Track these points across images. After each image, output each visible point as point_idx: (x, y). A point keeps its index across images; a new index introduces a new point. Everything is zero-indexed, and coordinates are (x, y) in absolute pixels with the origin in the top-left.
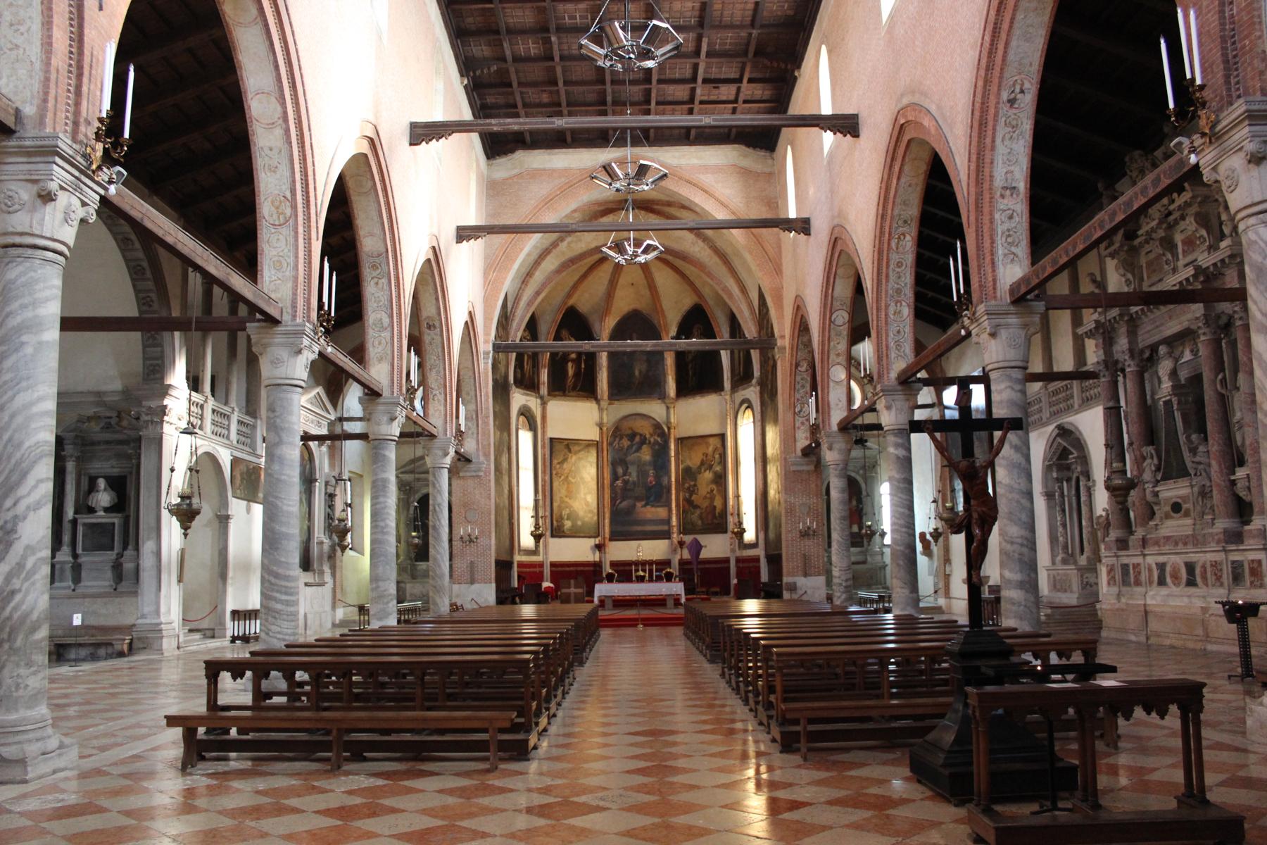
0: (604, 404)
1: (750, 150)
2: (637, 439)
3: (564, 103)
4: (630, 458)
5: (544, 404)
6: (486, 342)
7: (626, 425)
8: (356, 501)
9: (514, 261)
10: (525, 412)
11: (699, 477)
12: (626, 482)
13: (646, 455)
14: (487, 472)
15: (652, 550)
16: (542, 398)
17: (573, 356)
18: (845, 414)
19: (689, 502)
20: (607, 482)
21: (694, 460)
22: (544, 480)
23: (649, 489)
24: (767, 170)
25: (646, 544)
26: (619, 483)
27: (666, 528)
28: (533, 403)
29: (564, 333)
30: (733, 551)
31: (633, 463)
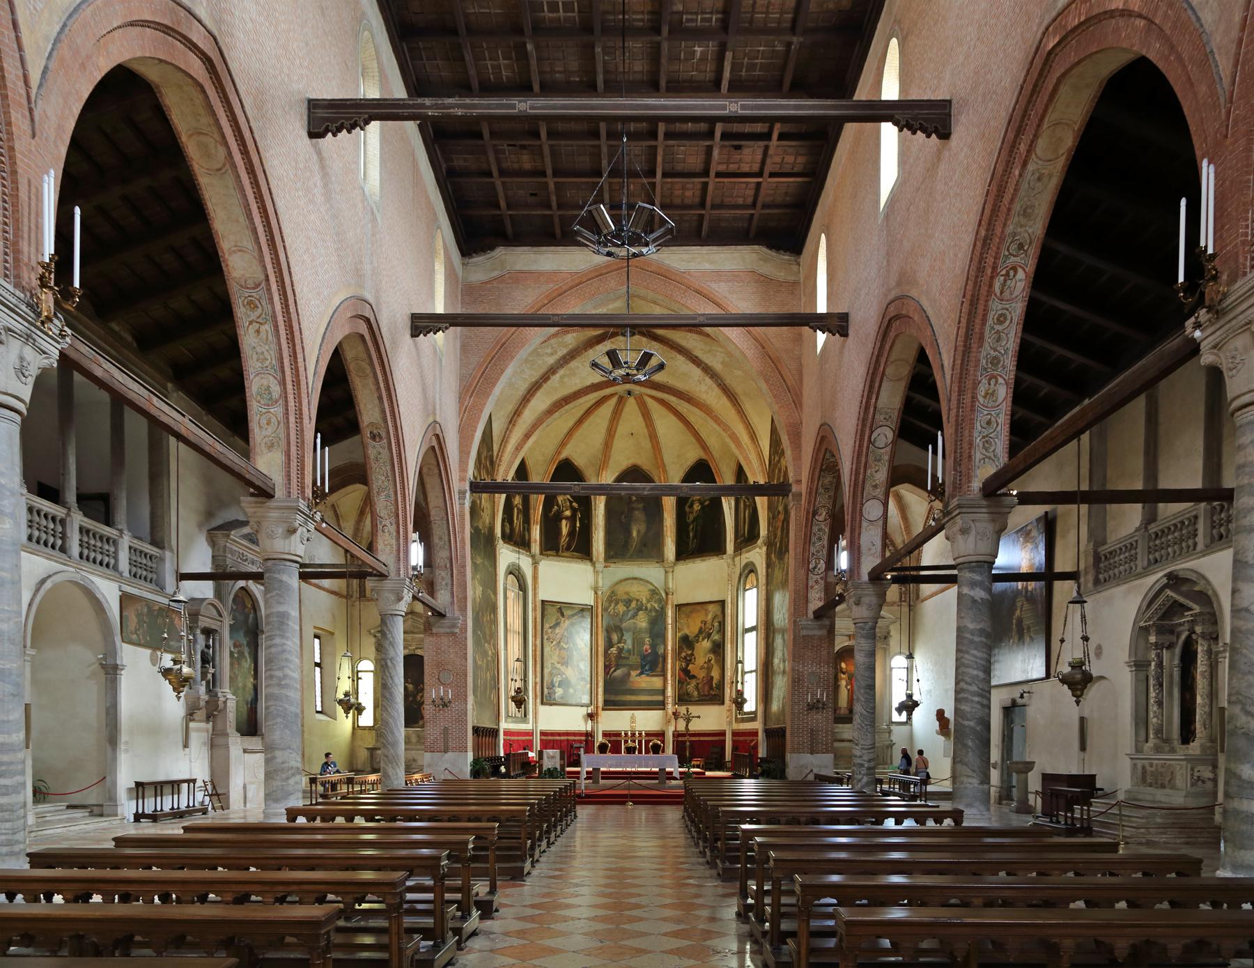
0: (600, 566)
1: (773, 253)
2: (633, 605)
3: (549, 172)
4: (624, 625)
5: (535, 564)
6: (462, 479)
7: (621, 590)
8: (327, 661)
9: (494, 385)
10: (515, 572)
11: (697, 645)
12: (620, 650)
13: (642, 622)
14: (464, 630)
15: (647, 721)
16: (533, 557)
17: (568, 513)
18: (879, 561)
19: (685, 671)
20: (601, 649)
21: (692, 628)
23: (644, 657)
24: (791, 278)
25: (639, 714)
26: (614, 650)
27: (660, 698)
28: (525, 563)
30: (730, 723)
31: (628, 630)
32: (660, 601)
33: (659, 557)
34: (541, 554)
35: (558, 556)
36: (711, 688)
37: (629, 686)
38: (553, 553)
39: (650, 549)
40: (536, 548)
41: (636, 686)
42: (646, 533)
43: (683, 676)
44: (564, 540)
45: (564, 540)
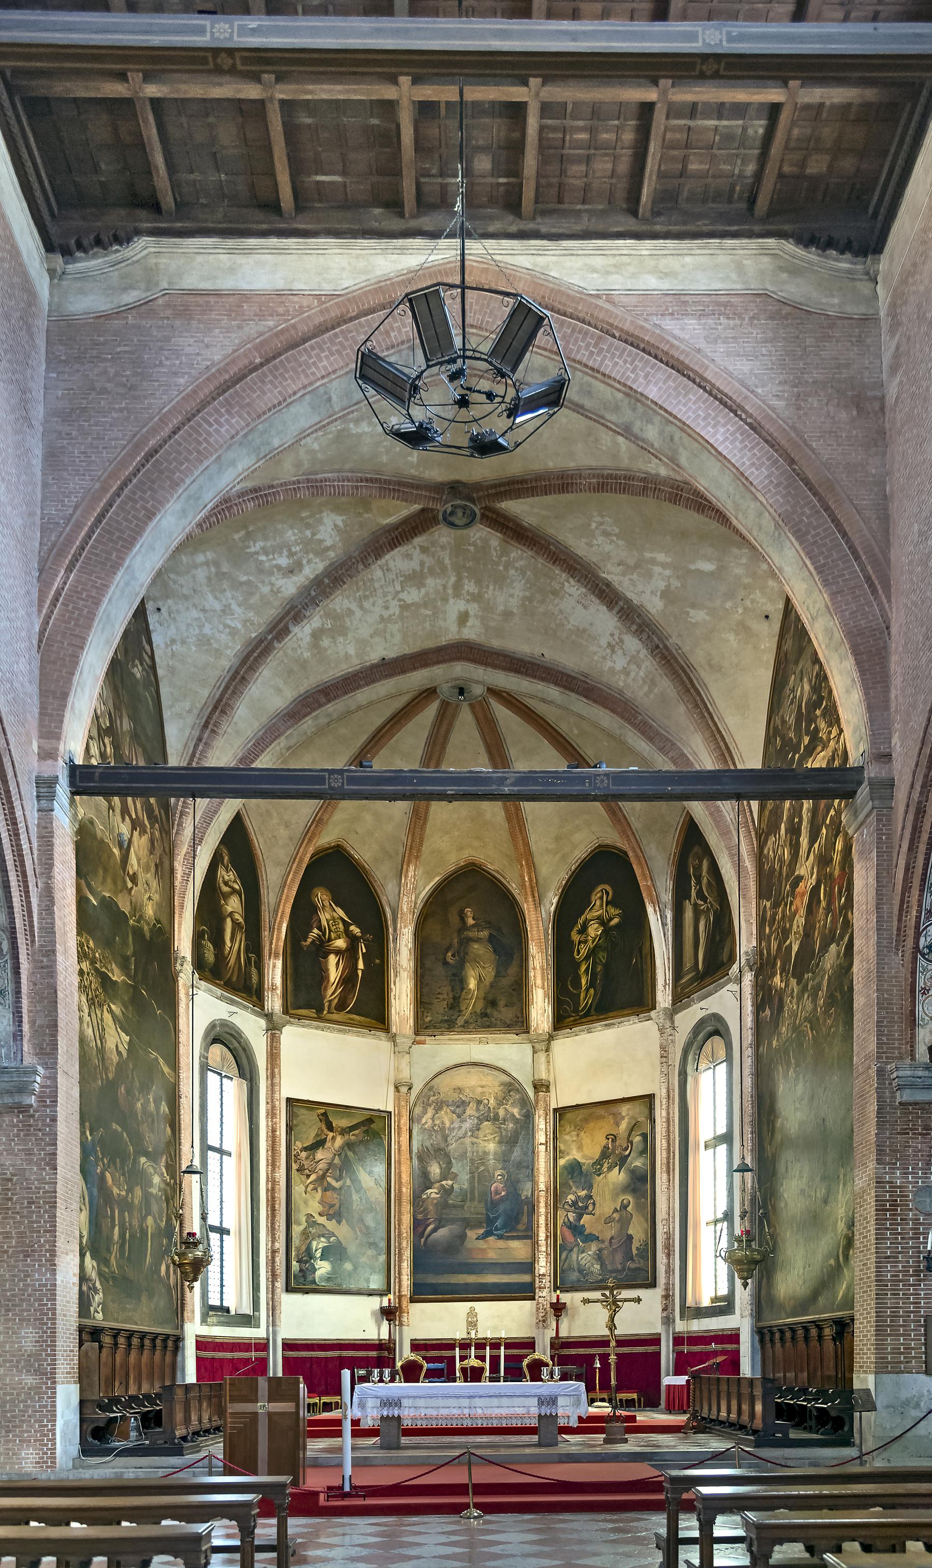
7: (446, 1084)
12: (447, 1192)
15: (502, 1319)
22: (272, 1181)
23: (493, 1205)
26: (433, 1193)
27: (526, 1278)
28: (251, 1027)
29: (321, 896)
30: (668, 1321)
33: (519, 1023)
34: (286, 1011)
35: (319, 1018)
36: (629, 1257)
37: (461, 1258)
41: (478, 1258)
44: (332, 992)
45: (332, 992)
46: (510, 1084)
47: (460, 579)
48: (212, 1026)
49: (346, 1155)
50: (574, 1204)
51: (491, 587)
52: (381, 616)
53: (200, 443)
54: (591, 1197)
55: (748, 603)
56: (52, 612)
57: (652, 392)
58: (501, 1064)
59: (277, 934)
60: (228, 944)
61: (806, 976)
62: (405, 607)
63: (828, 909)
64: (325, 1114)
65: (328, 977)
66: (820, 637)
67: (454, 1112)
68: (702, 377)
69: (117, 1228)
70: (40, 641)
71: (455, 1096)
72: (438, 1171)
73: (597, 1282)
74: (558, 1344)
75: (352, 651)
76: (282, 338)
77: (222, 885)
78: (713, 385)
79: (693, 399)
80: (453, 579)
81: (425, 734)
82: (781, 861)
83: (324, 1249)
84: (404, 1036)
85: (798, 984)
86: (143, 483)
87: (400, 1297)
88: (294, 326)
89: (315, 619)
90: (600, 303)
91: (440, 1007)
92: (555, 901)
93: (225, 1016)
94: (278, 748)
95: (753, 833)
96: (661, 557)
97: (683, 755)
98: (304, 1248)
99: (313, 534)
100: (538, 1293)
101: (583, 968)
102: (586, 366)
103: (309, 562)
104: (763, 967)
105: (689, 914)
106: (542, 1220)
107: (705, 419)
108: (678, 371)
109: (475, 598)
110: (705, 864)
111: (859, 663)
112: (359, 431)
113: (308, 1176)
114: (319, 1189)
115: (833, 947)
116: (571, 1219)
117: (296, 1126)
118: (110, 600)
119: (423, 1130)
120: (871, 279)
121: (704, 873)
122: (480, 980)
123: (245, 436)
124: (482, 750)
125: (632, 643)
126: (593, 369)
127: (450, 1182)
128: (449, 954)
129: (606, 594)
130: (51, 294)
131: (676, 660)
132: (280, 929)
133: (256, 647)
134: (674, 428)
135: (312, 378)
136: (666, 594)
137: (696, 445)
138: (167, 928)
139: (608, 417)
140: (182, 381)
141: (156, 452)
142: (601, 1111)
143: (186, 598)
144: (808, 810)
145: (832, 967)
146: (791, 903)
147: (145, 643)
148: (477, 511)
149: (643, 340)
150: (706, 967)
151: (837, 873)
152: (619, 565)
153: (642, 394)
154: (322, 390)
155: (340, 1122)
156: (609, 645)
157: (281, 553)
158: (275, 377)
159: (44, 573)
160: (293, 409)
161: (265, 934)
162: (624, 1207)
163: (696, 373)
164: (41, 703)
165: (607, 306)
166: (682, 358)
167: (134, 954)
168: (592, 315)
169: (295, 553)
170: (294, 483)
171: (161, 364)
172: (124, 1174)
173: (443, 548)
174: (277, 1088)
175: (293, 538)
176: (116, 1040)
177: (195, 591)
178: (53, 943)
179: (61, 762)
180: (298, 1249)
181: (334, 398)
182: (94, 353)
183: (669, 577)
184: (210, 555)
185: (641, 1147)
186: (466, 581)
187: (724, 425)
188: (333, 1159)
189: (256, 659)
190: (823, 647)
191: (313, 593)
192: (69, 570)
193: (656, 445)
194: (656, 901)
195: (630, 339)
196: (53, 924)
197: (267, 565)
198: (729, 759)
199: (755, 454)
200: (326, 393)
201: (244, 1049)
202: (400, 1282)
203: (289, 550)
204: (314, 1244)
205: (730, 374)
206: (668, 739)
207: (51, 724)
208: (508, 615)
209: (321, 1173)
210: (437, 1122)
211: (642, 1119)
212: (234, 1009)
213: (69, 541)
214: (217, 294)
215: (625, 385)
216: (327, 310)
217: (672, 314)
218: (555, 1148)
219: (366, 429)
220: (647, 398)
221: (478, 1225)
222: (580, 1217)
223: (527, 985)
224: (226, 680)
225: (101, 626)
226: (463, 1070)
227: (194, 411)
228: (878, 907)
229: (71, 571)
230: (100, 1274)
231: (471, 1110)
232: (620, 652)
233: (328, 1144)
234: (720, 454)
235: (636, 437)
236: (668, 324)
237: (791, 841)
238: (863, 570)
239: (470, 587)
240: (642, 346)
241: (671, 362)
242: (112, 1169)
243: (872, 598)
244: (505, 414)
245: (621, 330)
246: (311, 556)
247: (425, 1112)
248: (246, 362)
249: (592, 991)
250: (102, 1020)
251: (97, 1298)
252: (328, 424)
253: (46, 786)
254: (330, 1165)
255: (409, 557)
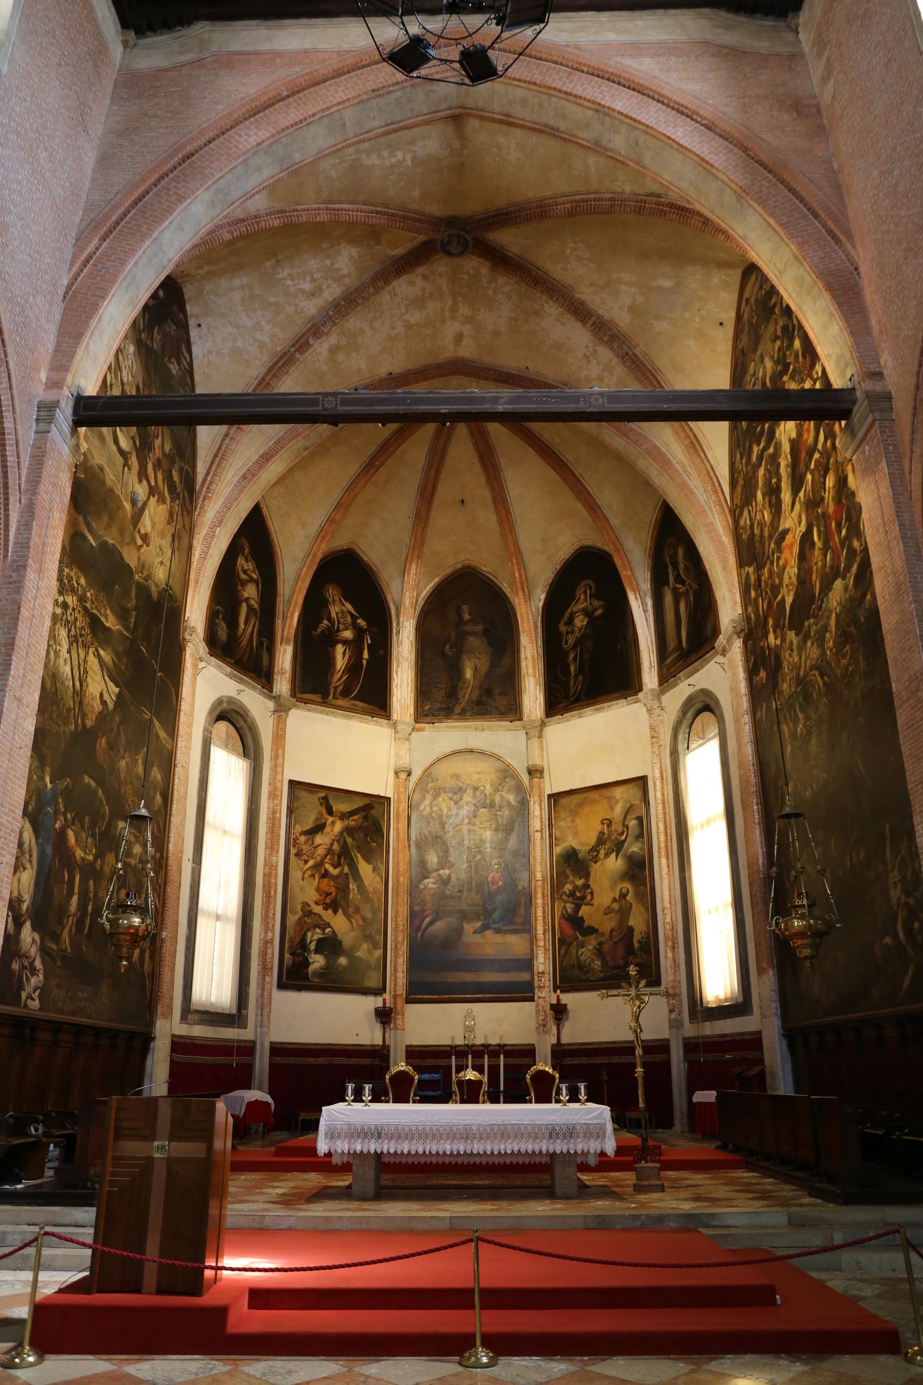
11: (595, 867)
12: (446, 881)
19: (575, 921)
21: (582, 833)
27: (525, 977)
32: (519, 788)
34: (293, 695)
38: (318, 698)
39: (497, 699)
40: (282, 685)
42: (487, 675)
43: (569, 930)
46: (506, 771)
47: (456, 303)
48: (219, 702)
49: (345, 841)
50: (572, 894)
51: (482, 310)
52: (389, 335)
53: (230, 149)
54: (588, 886)
55: (704, 312)
56: (82, 271)
57: (618, 106)
58: (496, 751)
59: (289, 621)
60: (242, 626)
61: (806, 624)
62: (409, 327)
63: (825, 549)
64: (325, 798)
65: (334, 665)
66: (790, 288)
67: (451, 799)
68: (659, 94)
69: (75, 899)
70: (66, 293)
71: (452, 783)
72: (435, 859)
73: (598, 980)
74: (560, 1053)
75: (363, 366)
76: (307, 78)
77: (241, 572)
78: (670, 100)
79: (654, 110)
80: (450, 303)
81: (426, 447)
82: (761, 525)
83: (319, 941)
84: (404, 723)
85: (797, 634)
86: (178, 177)
87: (395, 997)
88: (316, 71)
89: (332, 337)
90: (569, 49)
91: (439, 694)
92: (543, 597)
93: (233, 694)
94: (296, 447)
95: (727, 511)
96: (627, 277)
97: (655, 446)
98: (298, 939)
99: (333, 264)
100: (538, 994)
101: (571, 656)
102: (560, 91)
103: (328, 287)
104: (752, 633)
105: (668, 599)
106: (540, 913)
107: (665, 122)
108: (639, 92)
109: (470, 320)
110: (680, 552)
111: (835, 297)
112: (371, 162)
113: (306, 862)
114: (317, 876)
115: (838, 584)
116: (569, 911)
117: (297, 808)
118: (136, 263)
119: (421, 817)
120: (792, 31)
121: (680, 560)
122: (476, 670)
123: (270, 145)
124: (476, 460)
125: (605, 354)
126: (566, 93)
127: (447, 872)
128: (448, 646)
129: (580, 311)
130: (123, 58)
131: (644, 365)
132: (292, 617)
133: (281, 358)
134: (639, 132)
135: (329, 104)
136: (632, 309)
137: (659, 143)
138: (179, 597)
139: (580, 135)
140: (220, 107)
141: (193, 155)
142: (594, 795)
143: (223, 315)
144: (787, 466)
145: (839, 604)
146: (778, 558)
147: (184, 350)
148: (470, 240)
149: (607, 72)
150: (691, 641)
151: (831, 509)
152: (591, 285)
153: (609, 108)
154: (337, 115)
155: (340, 807)
156: (585, 356)
157: (304, 279)
158: (299, 104)
159: (81, 241)
160: (313, 129)
161: (279, 622)
162: (623, 896)
163: (655, 91)
164: (58, 342)
165: (576, 51)
166: (641, 82)
167: (136, 608)
168: (563, 58)
169: (317, 279)
170: (315, 210)
171: (205, 97)
172: (93, 835)
173: (441, 276)
174: (279, 769)
175: (315, 267)
176: (100, 688)
177: (230, 310)
178: (26, 557)
179: (66, 392)
180: (291, 941)
181: (348, 125)
182: (151, 92)
183: (634, 294)
184: (245, 280)
185: (637, 831)
186: (461, 306)
187: (683, 127)
188: (332, 845)
189: (280, 369)
190: (794, 296)
191: (331, 313)
192: (103, 239)
193: (623, 152)
194: (636, 590)
195: (596, 72)
196: (29, 539)
197: (293, 289)
198: (698, 446)
199: (712, 146)
200: (341, 119)
201: (250, 728)
202: (395, 980)
203: (312, 276)
204: (309, 934)
205: (684, 91)
206: (640, 434)
207: (63, 359)
208: (497, 333)
209: (319, 858)
210: (435, 809)
211: (636, 802)
212: (242, 687)
213: (107, 217)
214: (256, 53)
215: (594, 102)
216: (345, 60)
217: (630, 55)
218: (551, 836)
219: (376, 162)
220: (614, 110)
221: (477, 917)
222: (578, 908)
223: (519, 675)
224: (254, 385)
225: (125, 284)
226: (458, 758)
227: (228, 127)
228: (898, 514)
229: (104, 240)
230: (43, 950)
231: (467, 797)
232: (594, 362)
233: (327, 829)
234: (682, 146)
235: (606, 149)
236: (628, 61)
237: (770, 501)
238: (824, 225)
239: (464, 310)
240: (606, 76)
241: (632, 86)
242: (78, 826)
243: (837, 247)
244: (494, 21)
245: (589, 66)
246: (330, 282)
247: (423, 799)
248: (275, 93)
249: (581, 678)
250: (85, 661)
251: (33, 980)
252: (343, 148)
253: (47, 411)
254: (330, 851)
255: (412, 283)
